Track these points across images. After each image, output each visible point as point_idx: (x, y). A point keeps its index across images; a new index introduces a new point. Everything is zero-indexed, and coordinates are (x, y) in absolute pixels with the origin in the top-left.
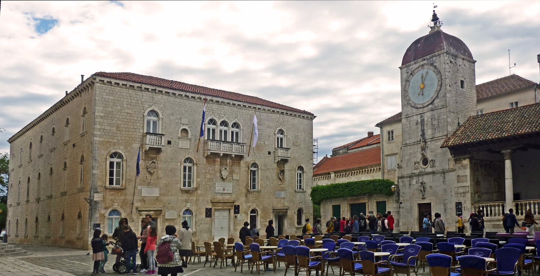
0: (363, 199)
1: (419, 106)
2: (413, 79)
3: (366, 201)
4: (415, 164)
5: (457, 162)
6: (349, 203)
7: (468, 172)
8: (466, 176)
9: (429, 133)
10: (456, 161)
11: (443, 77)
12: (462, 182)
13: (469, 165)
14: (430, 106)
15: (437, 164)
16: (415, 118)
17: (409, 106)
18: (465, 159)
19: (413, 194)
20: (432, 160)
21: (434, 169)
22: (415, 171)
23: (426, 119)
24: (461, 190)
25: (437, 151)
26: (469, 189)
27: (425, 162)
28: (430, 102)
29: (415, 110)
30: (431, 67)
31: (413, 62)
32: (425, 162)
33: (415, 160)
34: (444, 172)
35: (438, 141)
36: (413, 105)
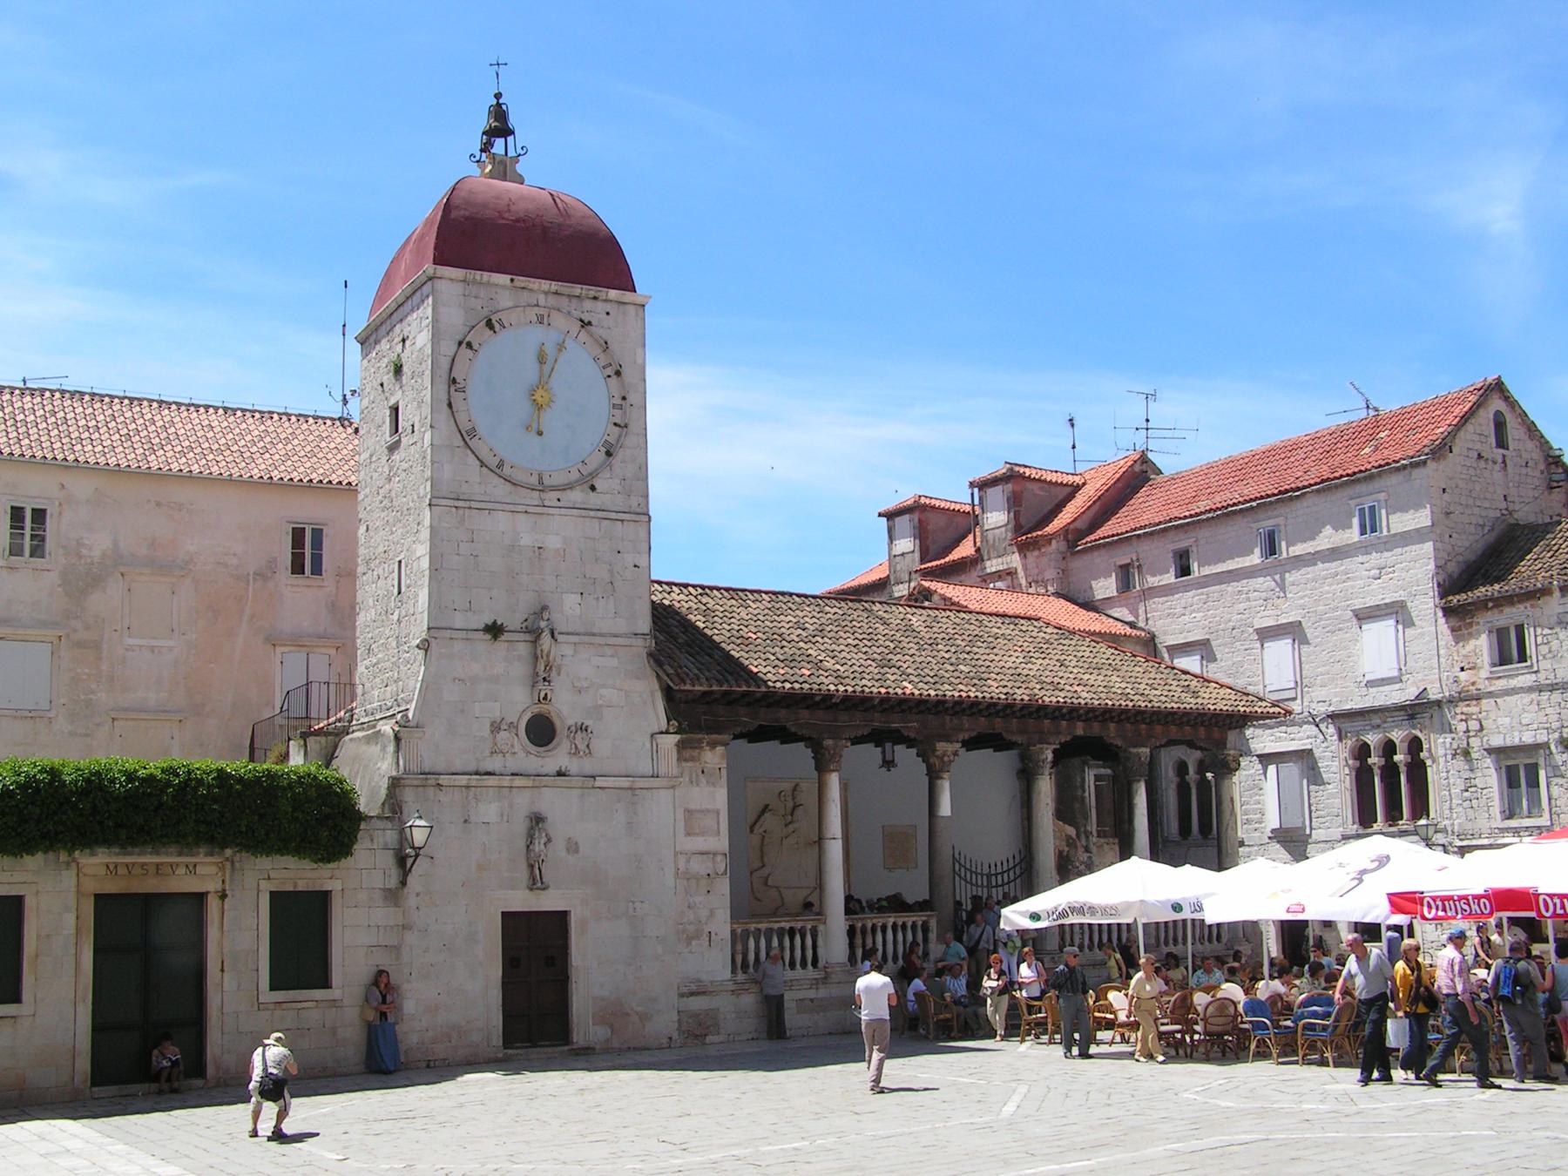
0: (192, 869)
1: (519, 476)
2: (492, 347)
3: (211, 886)
4: (496, 728)
5: (687, 753)
6: (92, 887)
7: (718, 797)
8: (718, 812)
9: (569, 608)
10: (681, 746)
11: (631, 398)
12: (702, 834)
13: (724, 772)
14: (576, 496)
15: (601, 746)
16: (502, 521)
17: (471, 459)
18: (713, 745)
19: (481, 868)
20: (583, 728)
21: (588, 766)
22: (495, 764)
23: (553, 542)
24: (699, 866)
25: (603, 691)
26: (721, 864)
27: (541, 731)
28: (575, 476)
29: (500, 490)
30: (583, 336)
31: (503, 279)
32: (541, 731)
33: (495, 711)
34: (633, 790)
35: (609, 651)
36: (493, 462)
